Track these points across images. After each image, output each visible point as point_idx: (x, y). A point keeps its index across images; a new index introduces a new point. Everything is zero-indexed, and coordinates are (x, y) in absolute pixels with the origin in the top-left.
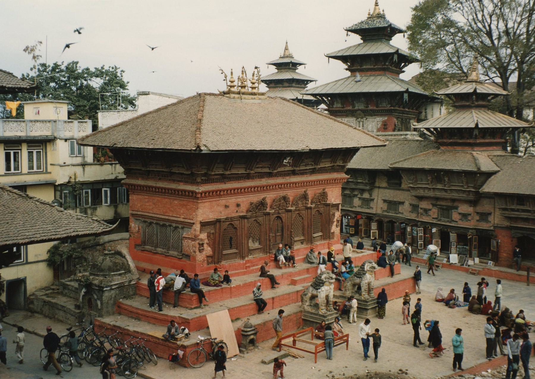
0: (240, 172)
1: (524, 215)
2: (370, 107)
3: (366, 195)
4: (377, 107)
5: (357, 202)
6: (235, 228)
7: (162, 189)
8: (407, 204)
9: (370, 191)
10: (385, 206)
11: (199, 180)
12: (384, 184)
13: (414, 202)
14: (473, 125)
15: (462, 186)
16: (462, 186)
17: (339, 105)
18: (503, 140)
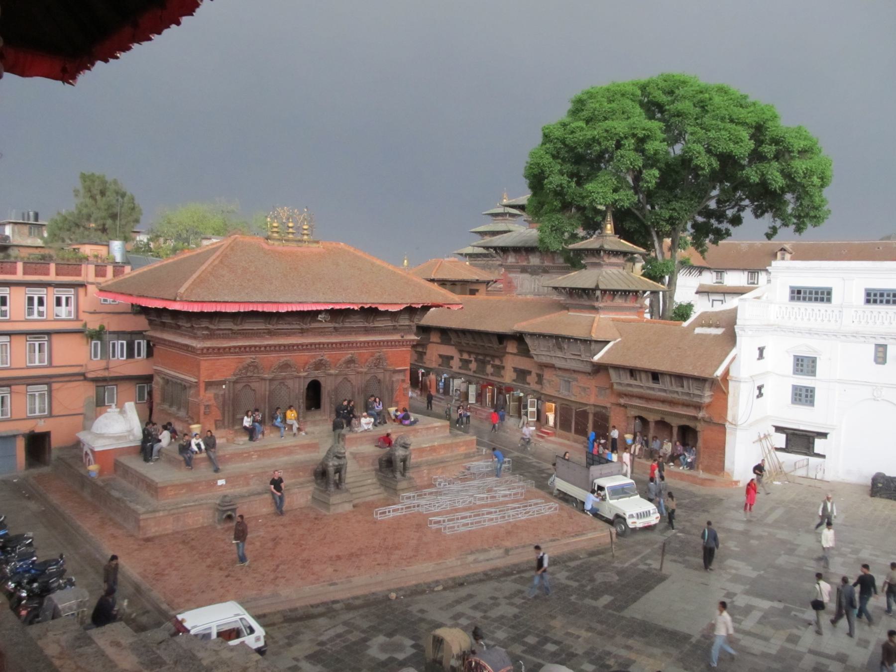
0: (255, 328)
1: (636, 390)
2: (546, 263)
3: (497, 362)
4: (554, 263)
5: (489, 369)
6: (254, 390)
7: (328, 345)
8: (534, 375)
9: (501, 358)
10: (514, 376)
11: (199, 333)
12: (515, 351)
13: (538, 372)
14: (593, 286)
15: (580, 355)
16: (580, 355)
17: (513, 260)
18: (638, 305)
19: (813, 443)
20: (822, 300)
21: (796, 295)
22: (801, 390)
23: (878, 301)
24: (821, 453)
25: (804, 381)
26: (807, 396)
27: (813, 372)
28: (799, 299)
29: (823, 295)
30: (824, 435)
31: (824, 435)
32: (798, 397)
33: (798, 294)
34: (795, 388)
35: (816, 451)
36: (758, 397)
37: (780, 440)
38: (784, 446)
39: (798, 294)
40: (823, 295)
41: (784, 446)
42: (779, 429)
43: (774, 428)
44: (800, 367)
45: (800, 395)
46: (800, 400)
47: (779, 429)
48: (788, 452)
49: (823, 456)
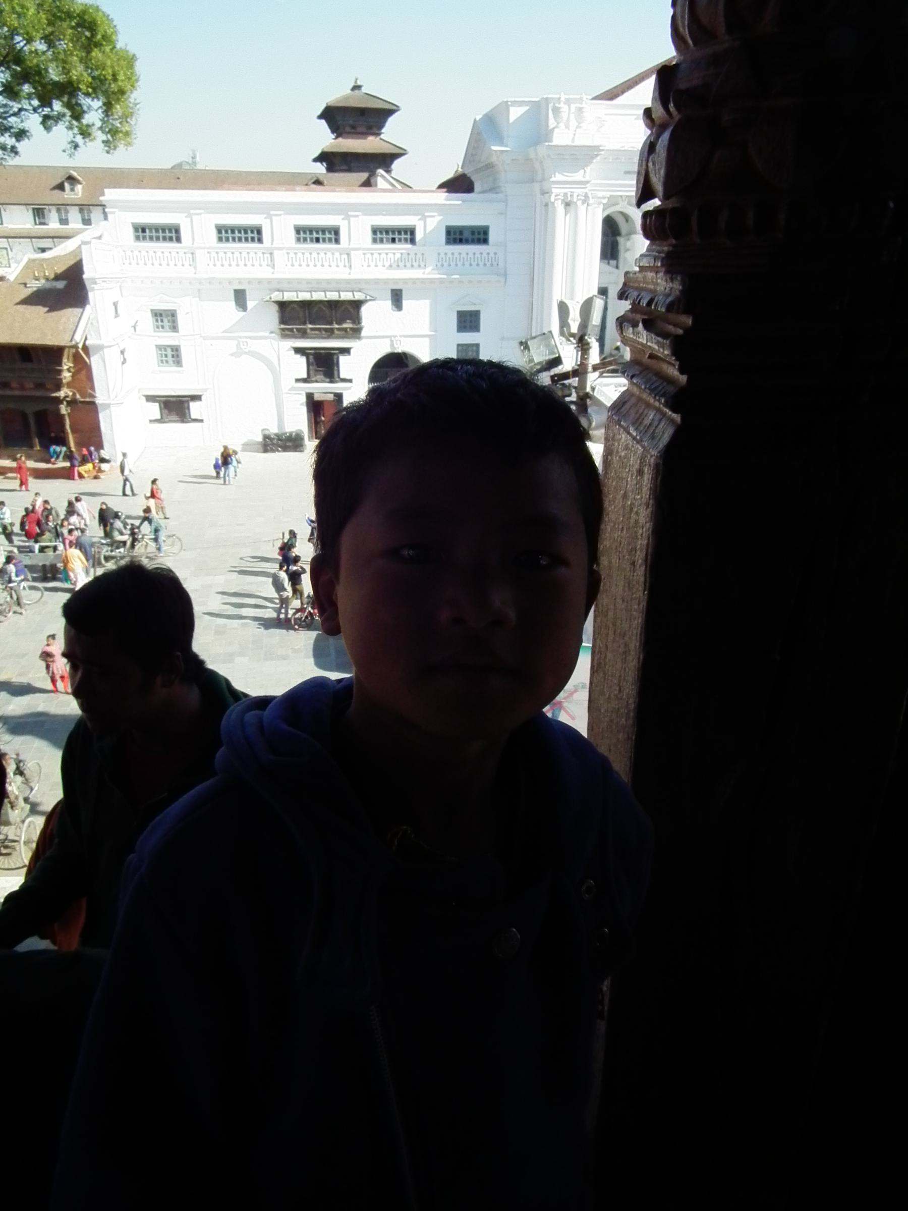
19: (188, 408)
20: (171, 239)
21: (140, 234)
22: (165, 350)
23: (231, 239)
24: (199, 418)
25: (169, 339)
26: (173, 356)
27: (174, 328)
28: (144, 238)
29: (171, 233)
30: (196, 398)
31: (196, 398)
32: (164, 358)
33: (142, 231)
34: (159, 348)
35: (193, 417)
36: (123, 363)
37: (155, 410)
38: (159, 417)
39: (142, 231)
40: (171, 233)
41: (159, 417)
42: (151, 398)
43: (144, 399)
44: (160, 323)
45: (166, 356)
46: (167, 362)
47: (151, 398)
48: (164, 422)
49: (201, 421)
